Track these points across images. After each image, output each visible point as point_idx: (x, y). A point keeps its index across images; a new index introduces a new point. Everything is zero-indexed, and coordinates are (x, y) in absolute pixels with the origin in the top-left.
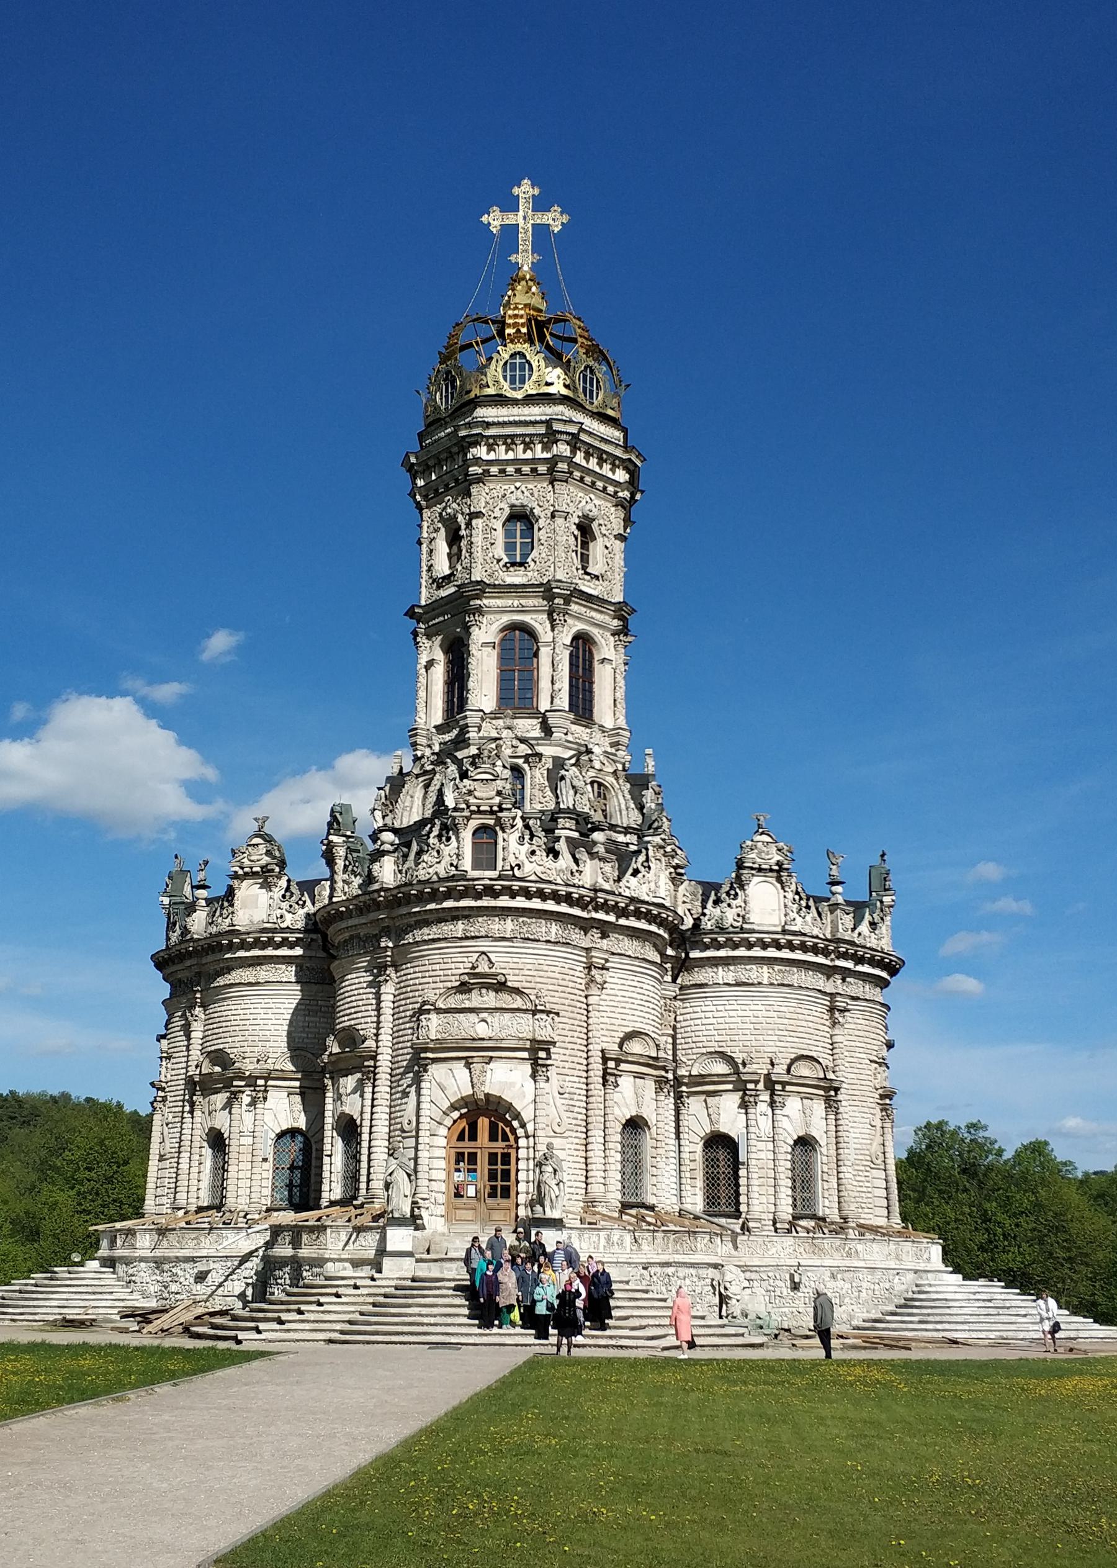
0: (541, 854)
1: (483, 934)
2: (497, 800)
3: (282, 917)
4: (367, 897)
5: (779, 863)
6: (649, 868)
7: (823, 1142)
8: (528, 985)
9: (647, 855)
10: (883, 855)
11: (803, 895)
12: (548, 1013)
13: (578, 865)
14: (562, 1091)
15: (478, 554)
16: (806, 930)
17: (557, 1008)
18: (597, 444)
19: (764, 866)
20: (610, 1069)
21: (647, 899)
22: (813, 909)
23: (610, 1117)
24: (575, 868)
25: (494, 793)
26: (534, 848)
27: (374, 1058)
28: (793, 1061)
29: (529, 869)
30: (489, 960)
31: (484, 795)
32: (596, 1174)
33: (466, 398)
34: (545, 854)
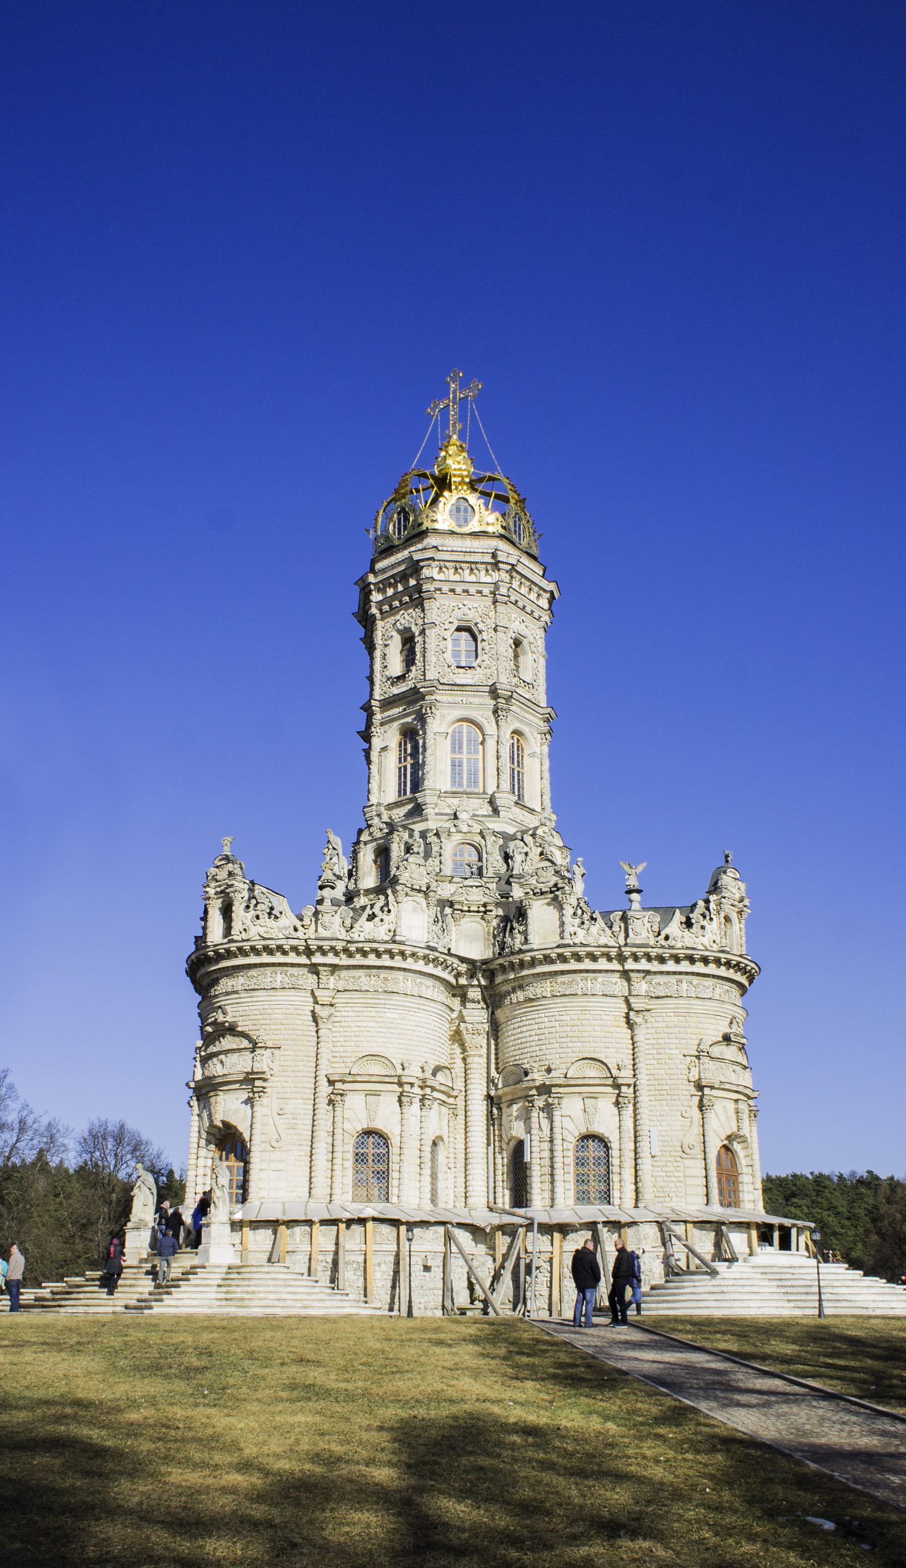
0: (264, 917)
5: (556, 885)
6: (389, 911)
8: (254, 1027)
16: (590, 940)
17: (278, 1044)
20: (337, 1089)
21: (388, 938)
24: (298, 924)
26: (259, 913)
29: (254, 931)
32: (321, 1179)
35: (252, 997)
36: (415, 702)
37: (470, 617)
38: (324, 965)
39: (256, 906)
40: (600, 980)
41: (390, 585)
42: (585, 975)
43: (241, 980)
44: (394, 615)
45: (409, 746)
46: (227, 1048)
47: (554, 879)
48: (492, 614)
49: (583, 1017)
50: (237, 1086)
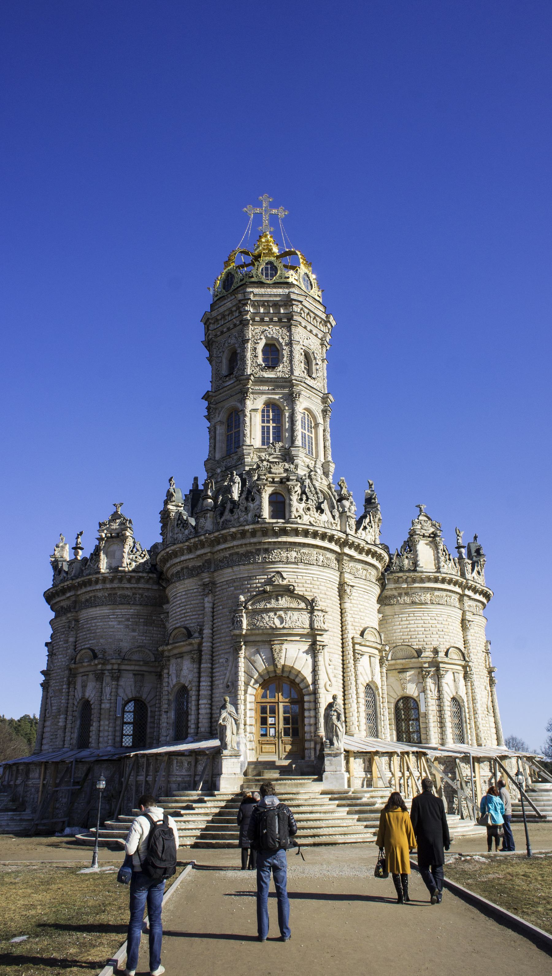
0: (313, 512)
1: (278, 560)
2: (285, 475)
3: (130, 564)
4: (197, 539)
6: (372, 527)
7: (465, 700)
9: (370, 519)
10: (476, 538)
11: (447, 552)
12: (322, 611)
13: (334, 519)
14: (331, 663)
15: (249, 362)
18: (313, 310)
19: (426, 534)
22: (452, 560)
23: (358, 682)
25: (282, 470)
26: (309, 506)
27: (200, 644)
28: (448, 650)
29: (306, 519)
30: (282, 576)
31: (277, 471)
33: (240, 284)
34: (315, 510)
35: (308, 569)
36: (284, 387)
37: (312, 347)
38: (348, 555)
39: (307, 500)
40: (453, 597)
41: (263, 306)
42: (449, 593)
43: (294, 554)
44: (263, 326)
45: (271, 414)
46: (285, 606)
47: (432, 530)
48: (320, 350)
49: (449, 620)
50: (298, 638)
